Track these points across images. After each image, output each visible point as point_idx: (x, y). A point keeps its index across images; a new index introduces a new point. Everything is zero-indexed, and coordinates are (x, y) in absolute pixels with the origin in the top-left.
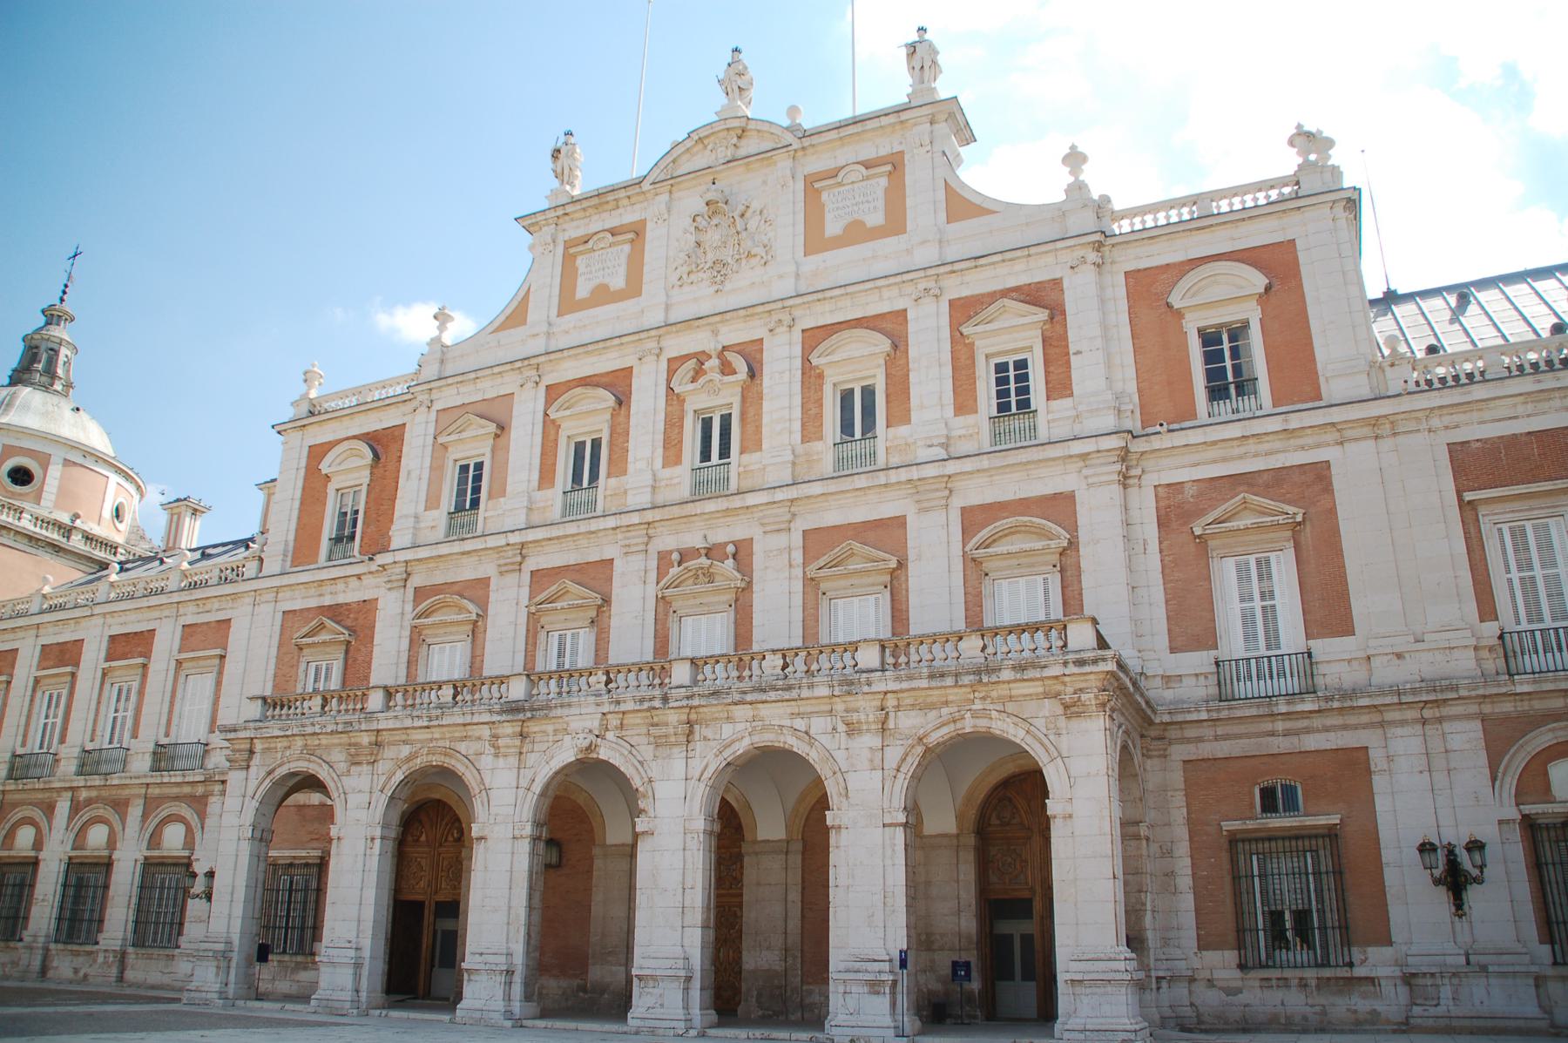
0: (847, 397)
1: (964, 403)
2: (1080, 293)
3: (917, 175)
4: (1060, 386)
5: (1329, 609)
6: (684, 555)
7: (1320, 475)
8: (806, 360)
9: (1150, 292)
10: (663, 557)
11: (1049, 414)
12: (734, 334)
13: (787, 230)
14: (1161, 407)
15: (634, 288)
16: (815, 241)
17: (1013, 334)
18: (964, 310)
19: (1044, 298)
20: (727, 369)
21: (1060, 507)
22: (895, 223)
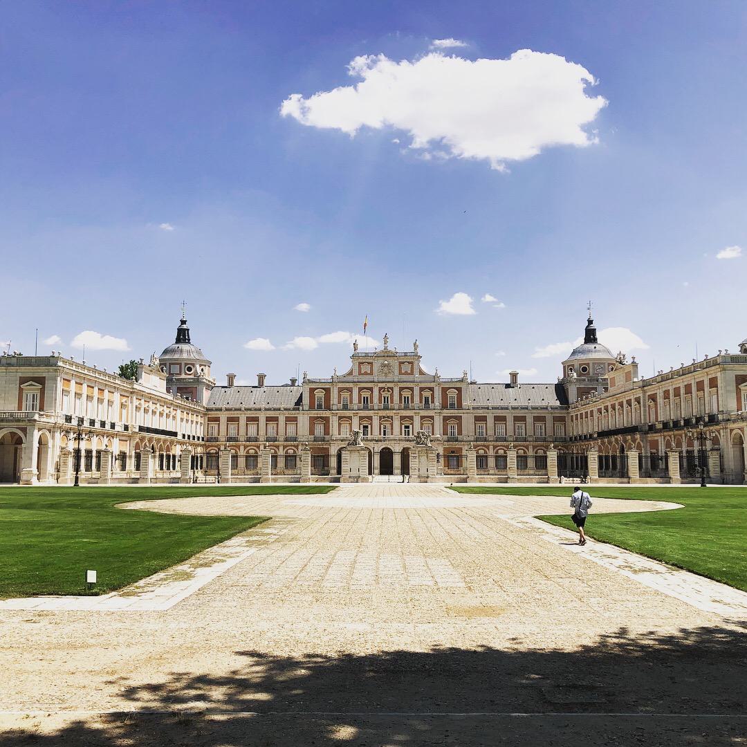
0: (405, 397)
1: (421, 402)
2: (436, 389)
3: (415, 366)
4: (433, 402)
5: (460, 432)
6: (384, 417)
7: (461, 416)
8: (400, 393)
9: (444, 390)
10: (380, 417)
11: (431, 406)
12: (389, 385)
13: (397, 372)
14: (444, 407)
15: (371, 374)
16: (400, 373)
17: (427, 394)
18: (422, 389)
19: (431, 389)
20: (389, 391)
21: (432, 418)
22: (412, 373)
